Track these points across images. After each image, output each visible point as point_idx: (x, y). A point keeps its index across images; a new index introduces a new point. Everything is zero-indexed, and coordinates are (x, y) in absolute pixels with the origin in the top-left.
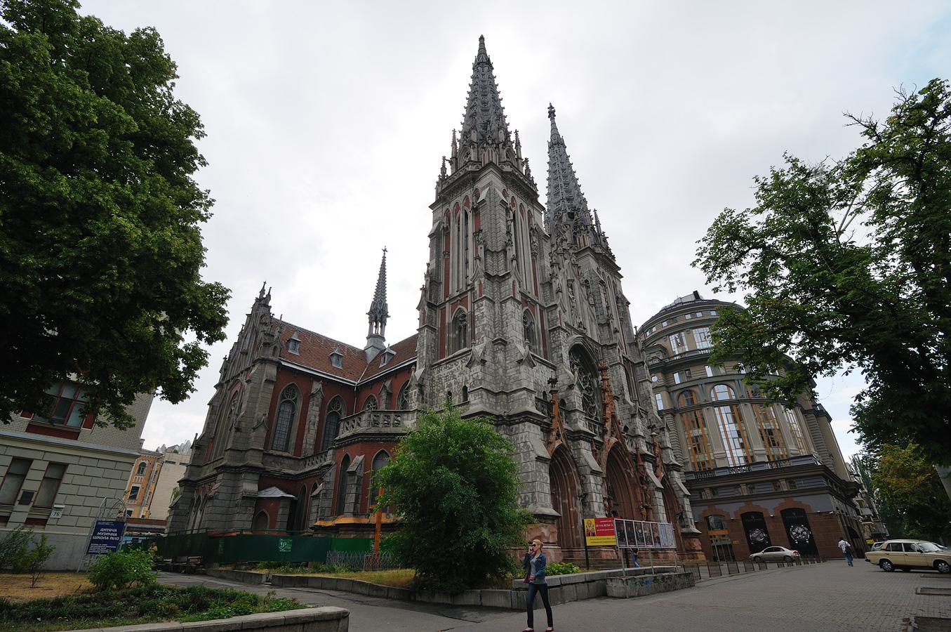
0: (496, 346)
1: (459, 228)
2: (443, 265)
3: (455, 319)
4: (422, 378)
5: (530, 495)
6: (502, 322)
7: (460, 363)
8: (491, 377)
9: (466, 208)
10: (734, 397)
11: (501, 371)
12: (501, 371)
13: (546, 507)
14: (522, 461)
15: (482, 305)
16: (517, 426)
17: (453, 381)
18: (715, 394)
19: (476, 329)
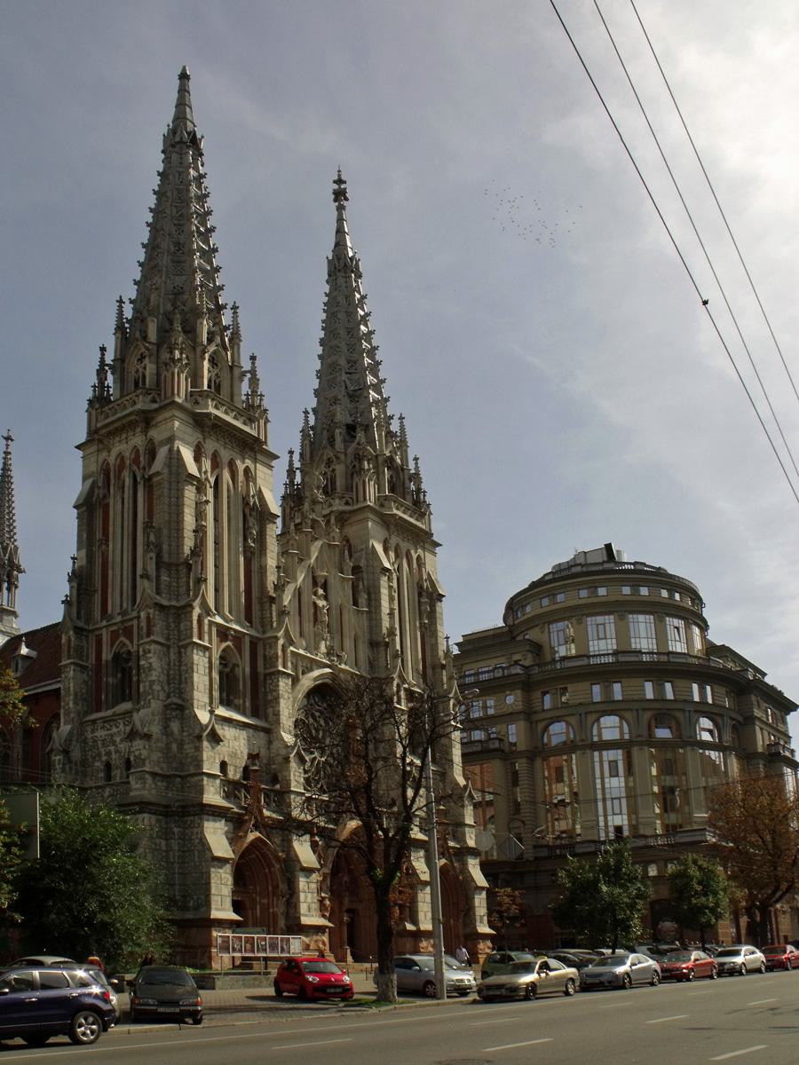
0: (169, 712)
1: (123, 499)
2: (98, 561)
3: (117, 657)
4: (69, 740)
5: (203, 897)
6: (180, 675)
7: (121, 727)
8: (160, 755)
9: (135, 468)
10: (627, 737)
11: (174, 746)
12: (174, 746)
13: (223, 910)
14: (196, 859)
15: (150, 652)
16: (192, 818)
17: (112, 748)
18: (600, 729)
19: (141, 685)
